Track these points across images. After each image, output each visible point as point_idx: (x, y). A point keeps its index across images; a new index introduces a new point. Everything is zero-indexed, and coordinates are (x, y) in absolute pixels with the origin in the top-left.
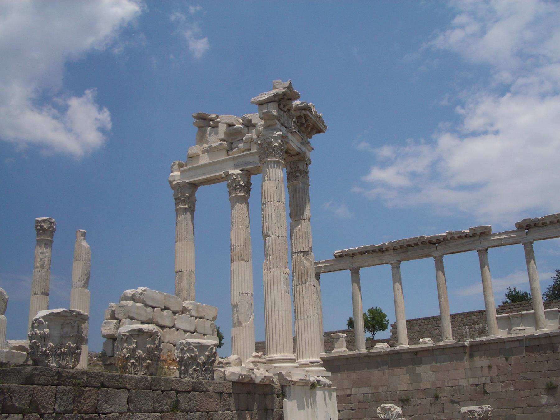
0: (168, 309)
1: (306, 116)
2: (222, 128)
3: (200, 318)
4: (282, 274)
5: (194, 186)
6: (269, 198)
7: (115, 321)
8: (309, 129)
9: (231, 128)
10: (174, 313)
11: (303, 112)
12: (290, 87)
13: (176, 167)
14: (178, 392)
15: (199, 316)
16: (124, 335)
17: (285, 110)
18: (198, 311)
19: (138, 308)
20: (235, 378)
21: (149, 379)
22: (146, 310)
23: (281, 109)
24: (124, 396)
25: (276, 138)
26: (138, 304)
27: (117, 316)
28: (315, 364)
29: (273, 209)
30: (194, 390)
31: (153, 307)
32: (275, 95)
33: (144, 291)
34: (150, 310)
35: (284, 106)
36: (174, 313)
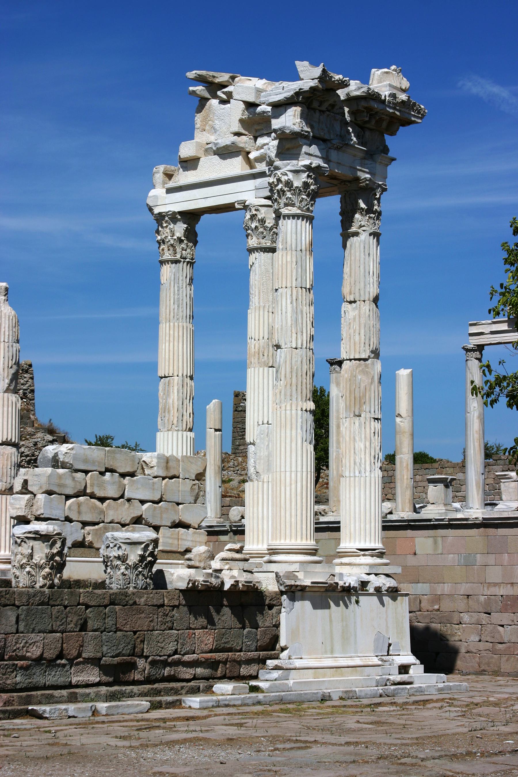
0: (112, 471)
1: (369, 110)
2: (235, 111)
3: (171, 478)
4: (300, 412)
5: (191, 217)
6: (284, 283)
7: (27, 496)
8: (384, 124)
9: (252, 110)
10: (123, 475)
11: (363, 104)
12: (324, 77)
13: (159, 177)
14: (87, 607)
15: (170, 474)
16: (19, 538)
17: (323, 108)
18: (167, 468)
19: (60, 477)
20: (183, 585)
21: (47, 592)
22: (74, 478)
23: (314, 110)
24: (11, 615)
25: (296, 172)
26: (61, 471)
27: (30, 488)
28: (367, 553)
29: (289, 301)
30: (112, 603)
31: (86, 472)
32: (297, 94)
33: (72, 449)
34: (80, 476)
35: (321, 103)
36: (123, 475)
